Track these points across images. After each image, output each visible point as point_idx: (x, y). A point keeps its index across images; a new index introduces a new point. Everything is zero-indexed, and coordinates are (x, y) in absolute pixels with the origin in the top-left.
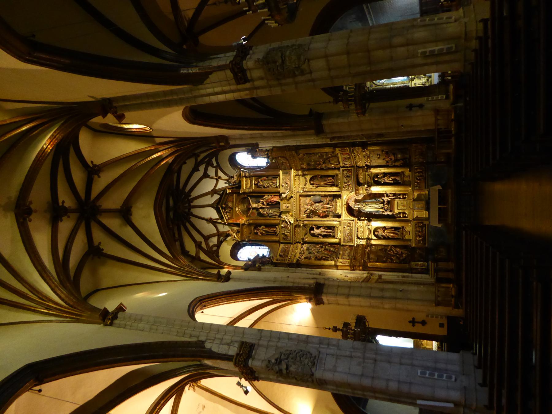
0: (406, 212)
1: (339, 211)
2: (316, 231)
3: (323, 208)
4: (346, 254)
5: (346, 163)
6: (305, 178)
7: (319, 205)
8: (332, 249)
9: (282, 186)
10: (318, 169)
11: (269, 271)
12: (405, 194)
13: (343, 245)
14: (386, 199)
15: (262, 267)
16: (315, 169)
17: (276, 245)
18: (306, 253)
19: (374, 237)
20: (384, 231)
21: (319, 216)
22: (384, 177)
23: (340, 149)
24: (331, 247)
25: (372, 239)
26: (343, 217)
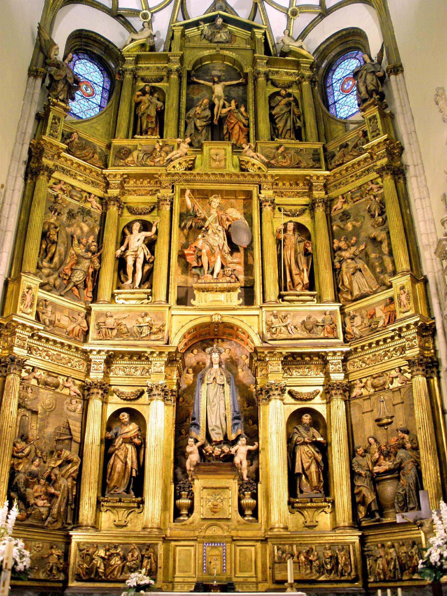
0: (196, 516)
1: (201, 299)
2: (137, 240)
3: (211, 253)
4: (58, 315)
5: (358, 321)
6: (302, 212)
7: (218, 239)
8: (78, 277)
9: (277, 148)
10: (332, 243)
11: (28, 96)
12: (255, 514)
13: (89, 311)
14: (241, 450)
15: (39, 81)
16: (332, 235)
17: (101, 128)
18: (74, 204)
19: (111, 410)
20: (130, 441)
21: (185, 246)
22: (316, 444)
23: (408, 287)
24: (86, 274)
25: (105, 403)
26: (180, 310)
